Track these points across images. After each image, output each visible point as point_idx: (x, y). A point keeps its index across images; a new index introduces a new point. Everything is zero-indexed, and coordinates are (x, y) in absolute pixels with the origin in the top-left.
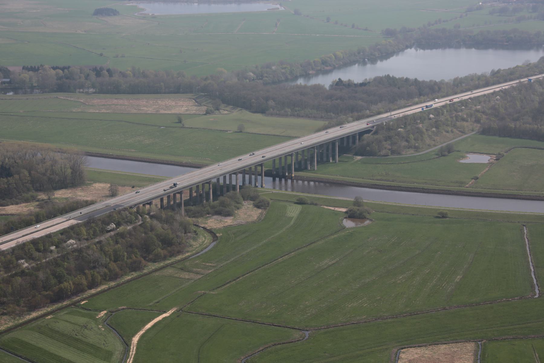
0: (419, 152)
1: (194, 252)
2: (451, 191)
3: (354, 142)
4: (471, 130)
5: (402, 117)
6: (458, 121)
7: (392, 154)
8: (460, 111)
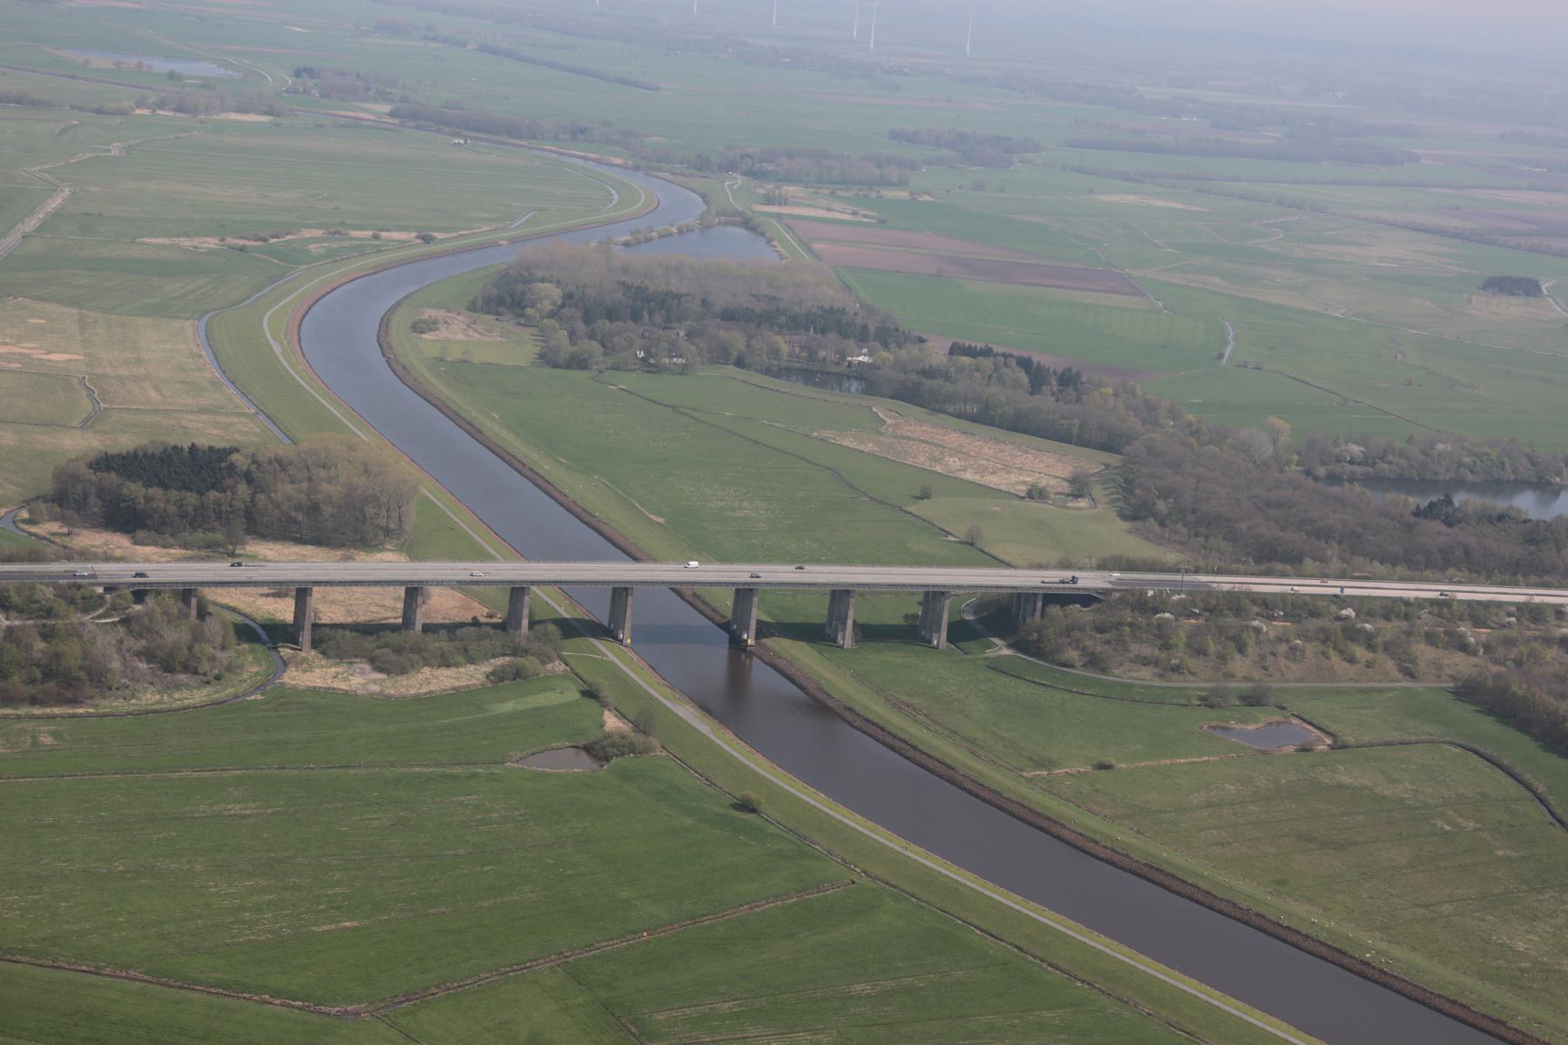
0: (1167, 681)
2: (953, 769)
3: (1033, 615)
4: (1452, 676)
6: (1437, 647)
7: (1084, 666)
8: (1495, 626)
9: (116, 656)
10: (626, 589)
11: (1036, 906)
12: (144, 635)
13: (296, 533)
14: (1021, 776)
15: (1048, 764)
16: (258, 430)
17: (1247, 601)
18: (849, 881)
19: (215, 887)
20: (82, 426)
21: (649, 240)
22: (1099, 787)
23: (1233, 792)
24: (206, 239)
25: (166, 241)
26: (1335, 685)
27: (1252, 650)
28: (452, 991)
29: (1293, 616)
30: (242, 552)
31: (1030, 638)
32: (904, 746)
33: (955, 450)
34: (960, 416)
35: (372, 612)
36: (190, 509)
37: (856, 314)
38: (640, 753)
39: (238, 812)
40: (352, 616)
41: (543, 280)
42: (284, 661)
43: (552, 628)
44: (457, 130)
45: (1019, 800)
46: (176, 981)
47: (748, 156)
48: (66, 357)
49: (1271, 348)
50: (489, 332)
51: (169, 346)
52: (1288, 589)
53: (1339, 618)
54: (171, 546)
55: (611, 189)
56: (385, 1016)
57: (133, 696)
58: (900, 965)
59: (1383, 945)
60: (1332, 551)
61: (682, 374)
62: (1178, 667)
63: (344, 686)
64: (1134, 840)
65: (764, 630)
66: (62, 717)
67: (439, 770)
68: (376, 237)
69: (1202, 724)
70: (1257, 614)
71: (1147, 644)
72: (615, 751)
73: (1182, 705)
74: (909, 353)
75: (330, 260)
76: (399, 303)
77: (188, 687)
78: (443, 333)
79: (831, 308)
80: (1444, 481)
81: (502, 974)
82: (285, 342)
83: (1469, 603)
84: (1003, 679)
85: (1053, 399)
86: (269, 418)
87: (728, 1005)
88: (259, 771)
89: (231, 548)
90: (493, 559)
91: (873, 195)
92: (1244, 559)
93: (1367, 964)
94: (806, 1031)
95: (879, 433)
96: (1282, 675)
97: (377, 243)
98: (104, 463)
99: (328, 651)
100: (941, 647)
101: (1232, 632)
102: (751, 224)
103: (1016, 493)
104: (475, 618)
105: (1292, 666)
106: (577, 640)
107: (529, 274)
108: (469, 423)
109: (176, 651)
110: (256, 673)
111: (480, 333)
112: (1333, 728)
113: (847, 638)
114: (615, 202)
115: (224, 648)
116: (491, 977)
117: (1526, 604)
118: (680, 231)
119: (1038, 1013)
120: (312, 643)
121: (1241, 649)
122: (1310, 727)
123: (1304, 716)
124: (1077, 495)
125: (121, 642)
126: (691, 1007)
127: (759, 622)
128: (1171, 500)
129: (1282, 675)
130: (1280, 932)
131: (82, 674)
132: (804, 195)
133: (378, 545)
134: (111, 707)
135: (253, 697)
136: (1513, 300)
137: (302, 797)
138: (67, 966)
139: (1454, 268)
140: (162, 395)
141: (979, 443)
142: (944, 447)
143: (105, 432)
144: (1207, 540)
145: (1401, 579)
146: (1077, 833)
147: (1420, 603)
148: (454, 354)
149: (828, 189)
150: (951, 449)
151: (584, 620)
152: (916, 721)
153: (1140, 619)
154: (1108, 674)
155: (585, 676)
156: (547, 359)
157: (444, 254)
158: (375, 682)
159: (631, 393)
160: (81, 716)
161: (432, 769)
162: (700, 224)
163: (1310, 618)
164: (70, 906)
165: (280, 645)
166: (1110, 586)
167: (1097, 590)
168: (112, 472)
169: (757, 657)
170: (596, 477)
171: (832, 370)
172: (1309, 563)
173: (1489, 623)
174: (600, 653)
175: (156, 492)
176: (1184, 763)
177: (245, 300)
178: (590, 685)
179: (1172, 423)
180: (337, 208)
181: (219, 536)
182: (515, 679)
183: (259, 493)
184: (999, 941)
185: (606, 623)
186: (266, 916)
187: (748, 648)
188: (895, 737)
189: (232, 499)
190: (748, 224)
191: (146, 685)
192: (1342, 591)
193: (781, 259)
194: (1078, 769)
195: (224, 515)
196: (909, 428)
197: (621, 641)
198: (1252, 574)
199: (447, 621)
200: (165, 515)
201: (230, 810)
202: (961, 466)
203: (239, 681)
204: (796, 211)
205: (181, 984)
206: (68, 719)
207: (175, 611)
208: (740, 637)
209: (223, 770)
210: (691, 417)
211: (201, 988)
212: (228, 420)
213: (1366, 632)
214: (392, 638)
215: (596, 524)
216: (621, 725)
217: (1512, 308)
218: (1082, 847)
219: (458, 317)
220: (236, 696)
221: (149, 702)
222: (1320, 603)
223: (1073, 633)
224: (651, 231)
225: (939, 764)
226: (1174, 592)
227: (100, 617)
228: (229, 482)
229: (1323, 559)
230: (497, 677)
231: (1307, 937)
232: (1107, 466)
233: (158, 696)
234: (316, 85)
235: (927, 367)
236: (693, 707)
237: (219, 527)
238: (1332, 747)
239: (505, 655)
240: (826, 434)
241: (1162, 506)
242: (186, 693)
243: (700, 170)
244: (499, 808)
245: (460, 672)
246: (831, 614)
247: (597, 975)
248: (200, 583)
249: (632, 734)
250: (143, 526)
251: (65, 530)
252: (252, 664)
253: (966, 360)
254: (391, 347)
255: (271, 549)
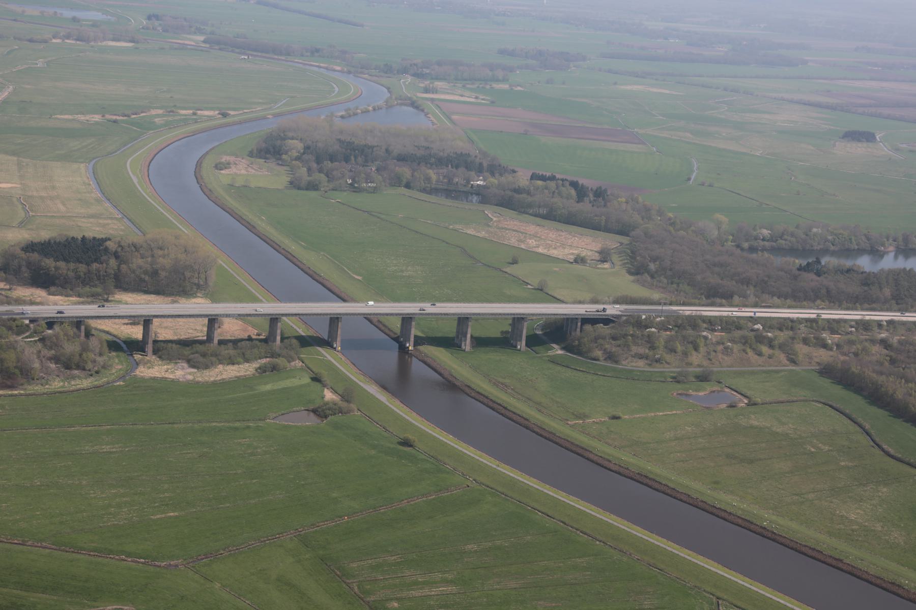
1: (28, 392)
4: (817, 363)
5: (689, 316)
6: (809, 346)
8: (843, 333)
9: (37, 360)
10: (338, 318)
11: (574, 498)
12: (53, 348)
13: (145, 287)
14: (568, 424)
15: (583, 416)
16: (123, 228)
17: (700, 321)
18: (466, 486)
19: (94, 494)
20: (19, 226)
21: (355, 114)
22: (612, 429)
23: (690, 431)
24: (94, 116)
25: (70, 117)
26: (750, 369)
27: (702, 349)
28: (232, 552)
29: (727, 329)
30: (113, 299)
31: (574, 344)
32: (499, 407)
33: (533, 235)
34: (536, 215)
35: (189, 333)
36: (82, 274)
37: (476, 157)
38: (345, 413)
39: (108, 450)
40: (177, 336)
41: (292, 138)
42: (137, 362)
43: (294, 341)
44: (243, 51)
45: (566, 438)
46: (70, 549)
47: (415, 64)
48: (9, 185)
49: (719, 174)
50: (260, 169)
51: (71, 179)
52: (725, 314)
53: (753, 330)
54: (71, 296)
55: (333, 84)
56: (193, 567)
57: (47, 384)
58: (494, 533)
59: (774, 518)
60: (750, 291)
61: (374, 193)
62: (659, 359)
63: (171, 376)
64: (631, 460)
65: (419, 341)
66: (5, 396)
67: (227, 424)
68: (194, 114)
69: (672, 392)
70: (706, 328)
71: (641, 347)
72: (331, 412)
73: (661, 381)
74: (507, 179)
75: (167, 128)
76: (207, 153)
77: (79, 377)
78: (233, 170)
79: (462, 153)
80: (817, 250)
81: (262, 542)
82: (140, 176)
83: (828, 320)
84: (559, 368)
85: (591, 205)
86: (130, 220)
87: (393, 558)
88: (121, 426)
89: (106, 296)
90: (261, 301)
91: (488, 87)
92: (699, 297)
93: (765, 528)
94: (439, 572)
95: (489, 226)
96: (720, 363)
97: (195, 117)
98: (30, 247)
99: (163, 356)
100: (522, 350)
101: (691, 339)
102: (416, 104)
103: (568, 260)
104: (249, 336)
105: (726, 358)
106: (309, 348)
107: (284, 135)
108: (248, 222)
109: (72, 357)
110: (121, 369)
111: (254, 169)
112: (749, 393)
113: (467, 345)
114: (336, 92)
115: (101, 355)
116: (255, 544)
117: (861, 320)
118: (374, 109)
119: (574, 560)
120: (153, 351)
121: (696, 349)
122: (735, 393)
123: (732, 387)
124: (603, 261)
125: (40, 352)
126: (372, 559)
127: (416, 337)
128: (658, 263)
129: (720, 363)
130: (715, 511)
131: (17, 371)
132: (447, 87)
133: (193, 294)
134: (34, 390)
135: (118, 383)
136: (860, 145)
137: (146, 441)
138: (5, 541)
139: (827, 126)
140: (66, 207)
141: (546, 232)
142: (526, 234)
143: (32, 230)
144: (678, 286)
145: (789, 307)
146: (599, 456)
147: (800, 321)
148: (239, 182)
149: (461, 83)
150: (530, 235)
151: (313, 336)
152: (506, 393)
153: (638, 332)
154: (617, 365)
155: (314, 370)
156: (294, 184)
157: (234, 124)
158: (190, 374)
159: (344, 204)
160: (16, 395)
161: (223, 424)
162: (386, 105)
163: (736, 330)
164: (8, 506)
165: (134, 353)
166: (620, 313)
167: (613, 316)
168: (35, 252)
169: (415, 357)
170: (322, 253)
171: (462, 190)
172: (736, 299)
173: (840, 332)
174: (323, 355)
175: (62, 264)
176: (662, 415)
177: (116, 152)
178: (316, 374)
179: (659, 218)
180: (171, 97)
181: (99, 290)
182: (272, 371)
183: (123, 264)
184: (552, 519)
185: (326, 338)
186: (124, 510)
187: (410, 352)
188: (494, 402)
189: (106, 268)
190: (414, 104)
191: (55, 377)
192: (755, 314)
193: (433, 125)
194: (601, 419)
195: (102, 278)
196: (506, 223)
197: (335, 348)
198: (703, 305)
199: (233, 338)
200: (66, 277)
201: (103, 449)
202: (536, 245)
203: (110, 374)
204: (443, 97)
205: (73, 550)
206: (8, 397)
207: (71, 333)
208: (405, 345)
209: (99, 426)
210: (378, 218)
211: (84, 552)
212: (106, 222)
213: (769, 338)
214: (200, 348)
215: (321, 280)
216: (334, 397)
217: (859, 149)
218: (602, 464)
219: (242, 161)
220: (108, 383)
221: (57, 387)
222: (742, 322)
223: (598, 341)
224: (357, 109)
225: (519, 418)
226: (657, 316)
227: (27, 337)
228: (104, 258)
229: (745, 296)
230: (262, 370)
231: (730, 513)
232: (621, 244)
233: (62, 384)
234: (160, 25)
235: (517, 187)
236: (376, 386)
237: (99, 285)
238: (748, 405)
239: (266, 357)
240: (457, 227)
241: (652, 267)
242: (78, 381)
243: (386, 73)
244: (262, 446)
245: (240, 368)
246: (458, 332)
247: (318, 541)
248: (86, 317)
249: (341, 402)
250: (54, 284)
251: (8, 287)
252: (117, 364)
253: (540, 183)
254: (202, 179)
255: (130, 297)
